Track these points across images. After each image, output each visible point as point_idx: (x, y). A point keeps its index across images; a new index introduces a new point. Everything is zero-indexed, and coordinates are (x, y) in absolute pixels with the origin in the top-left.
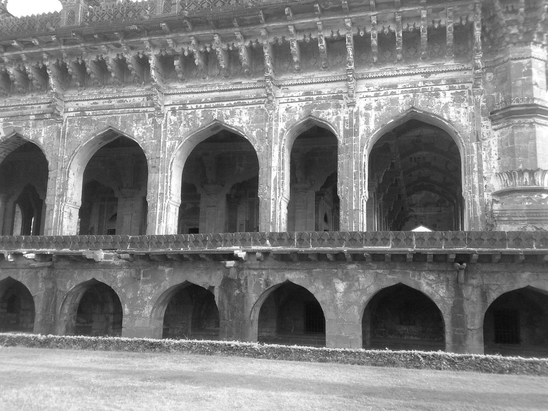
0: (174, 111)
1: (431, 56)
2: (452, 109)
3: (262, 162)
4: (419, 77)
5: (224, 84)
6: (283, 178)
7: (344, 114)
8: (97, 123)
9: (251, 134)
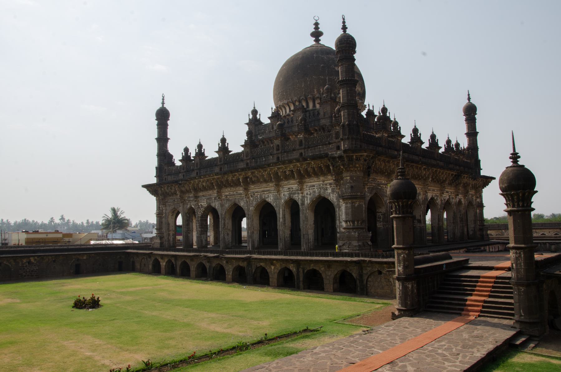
0: (252, 196)
1: (324, 174)
2: (331, 195)
3: (278, 215)
4: (321, 182)
5: (264, 185)
6: (285, 220)
7: (300, 197)
8: (231, 200)
9: (274, 205)
